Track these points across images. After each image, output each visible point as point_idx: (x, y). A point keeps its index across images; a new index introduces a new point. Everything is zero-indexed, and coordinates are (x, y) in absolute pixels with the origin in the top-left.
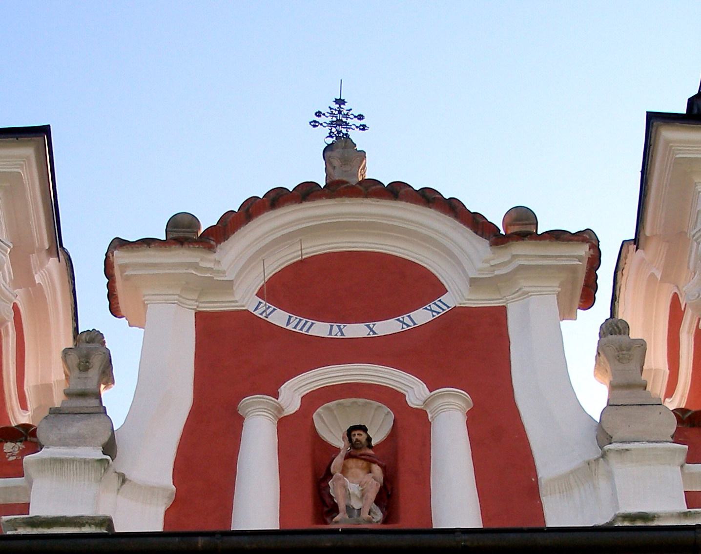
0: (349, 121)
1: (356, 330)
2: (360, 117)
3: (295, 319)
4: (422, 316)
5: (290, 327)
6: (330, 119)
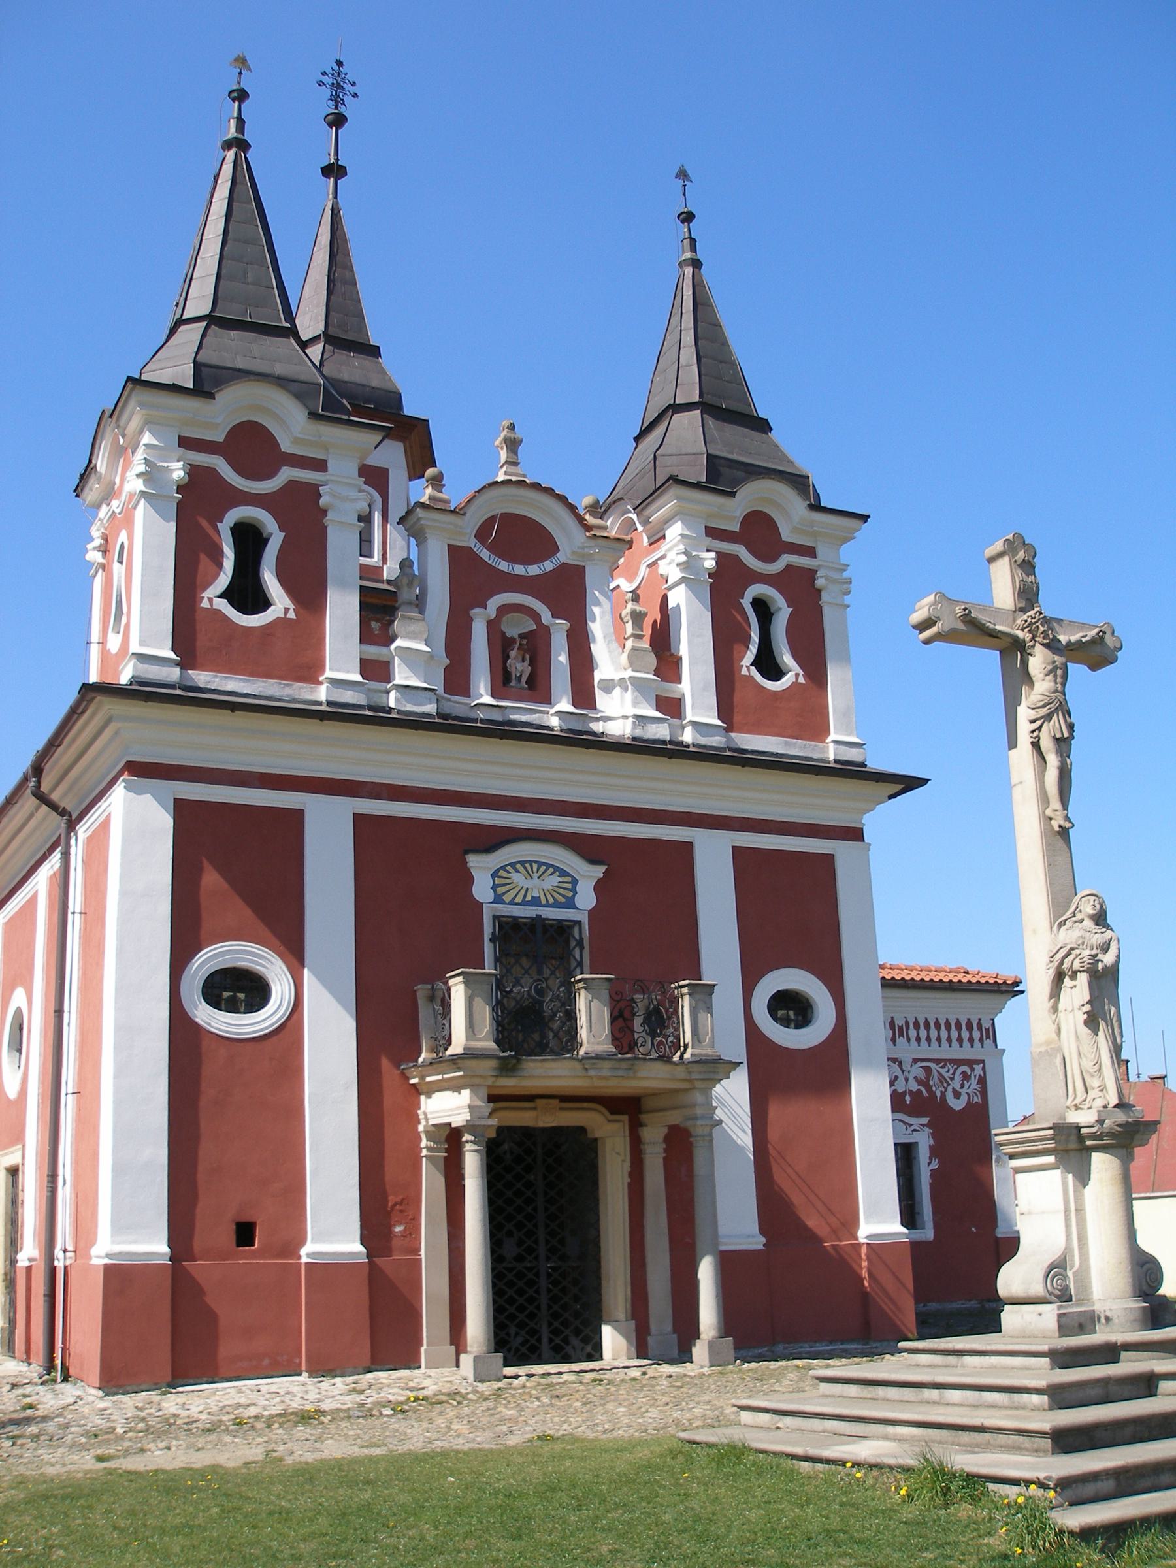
0: (345, 86)
1: (519, 570)
2: (353, 84)
3: (492, 557)
4: (548, 566)
5: (490, 562)
6: (330, 81)
